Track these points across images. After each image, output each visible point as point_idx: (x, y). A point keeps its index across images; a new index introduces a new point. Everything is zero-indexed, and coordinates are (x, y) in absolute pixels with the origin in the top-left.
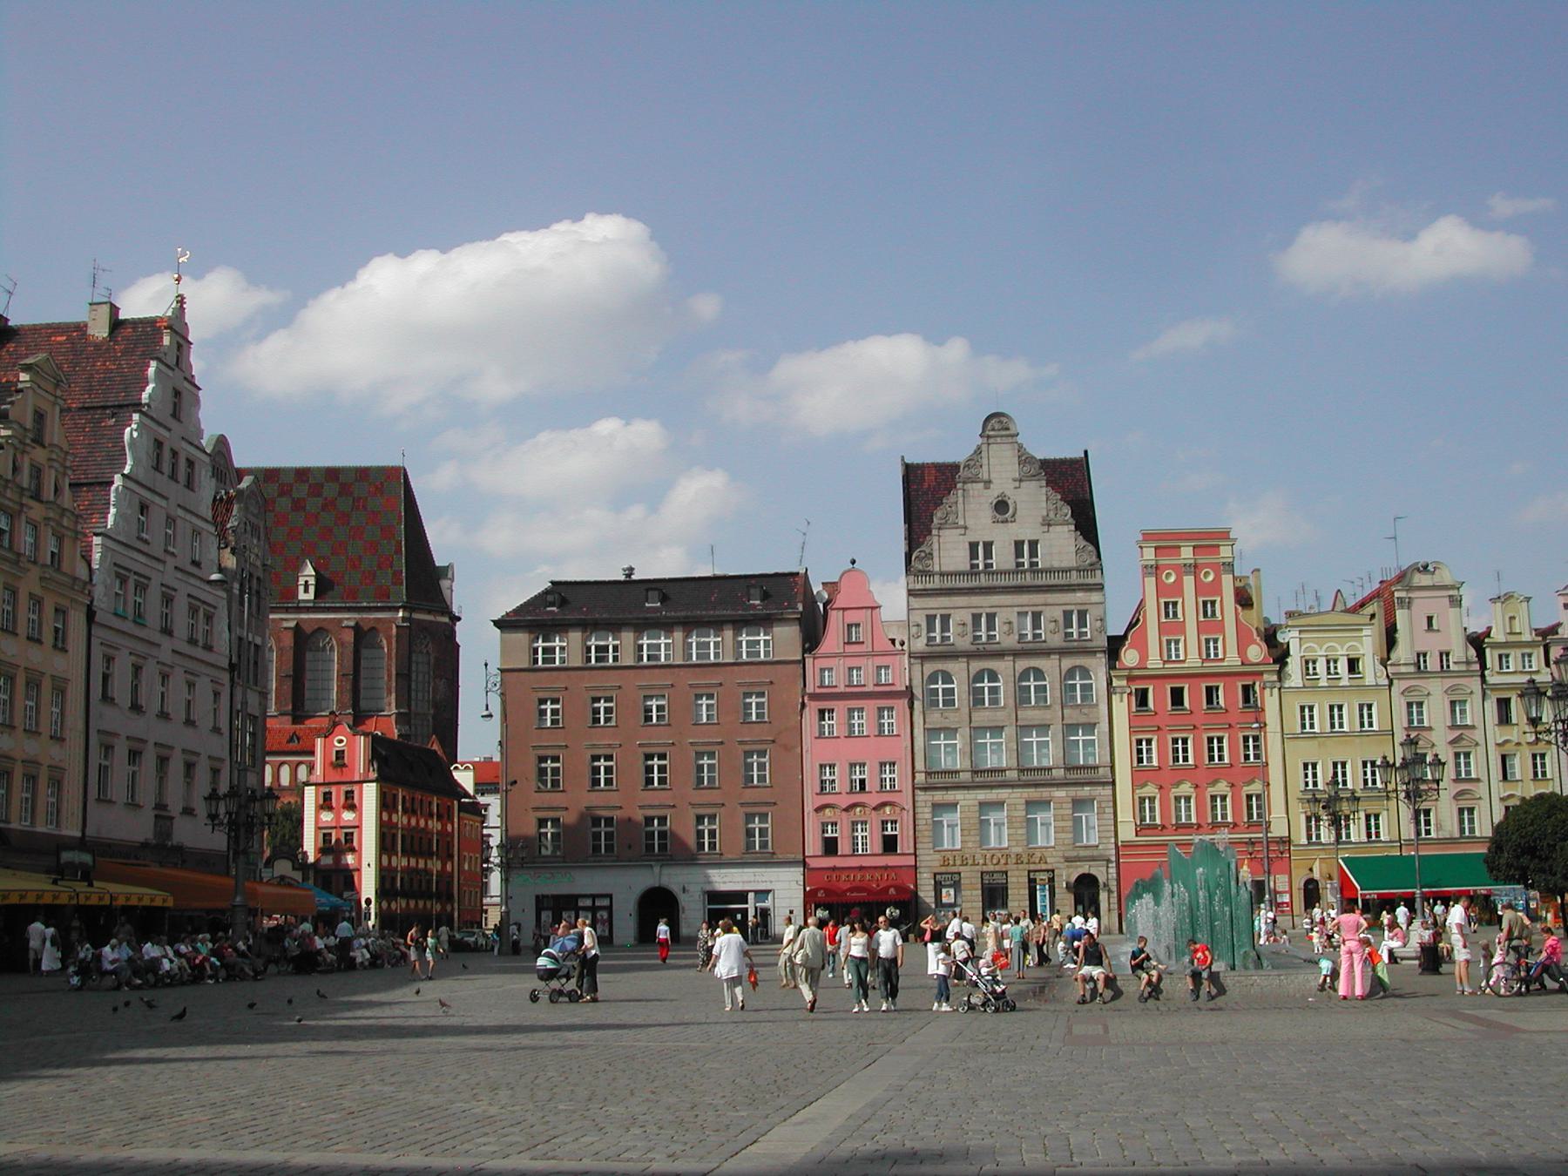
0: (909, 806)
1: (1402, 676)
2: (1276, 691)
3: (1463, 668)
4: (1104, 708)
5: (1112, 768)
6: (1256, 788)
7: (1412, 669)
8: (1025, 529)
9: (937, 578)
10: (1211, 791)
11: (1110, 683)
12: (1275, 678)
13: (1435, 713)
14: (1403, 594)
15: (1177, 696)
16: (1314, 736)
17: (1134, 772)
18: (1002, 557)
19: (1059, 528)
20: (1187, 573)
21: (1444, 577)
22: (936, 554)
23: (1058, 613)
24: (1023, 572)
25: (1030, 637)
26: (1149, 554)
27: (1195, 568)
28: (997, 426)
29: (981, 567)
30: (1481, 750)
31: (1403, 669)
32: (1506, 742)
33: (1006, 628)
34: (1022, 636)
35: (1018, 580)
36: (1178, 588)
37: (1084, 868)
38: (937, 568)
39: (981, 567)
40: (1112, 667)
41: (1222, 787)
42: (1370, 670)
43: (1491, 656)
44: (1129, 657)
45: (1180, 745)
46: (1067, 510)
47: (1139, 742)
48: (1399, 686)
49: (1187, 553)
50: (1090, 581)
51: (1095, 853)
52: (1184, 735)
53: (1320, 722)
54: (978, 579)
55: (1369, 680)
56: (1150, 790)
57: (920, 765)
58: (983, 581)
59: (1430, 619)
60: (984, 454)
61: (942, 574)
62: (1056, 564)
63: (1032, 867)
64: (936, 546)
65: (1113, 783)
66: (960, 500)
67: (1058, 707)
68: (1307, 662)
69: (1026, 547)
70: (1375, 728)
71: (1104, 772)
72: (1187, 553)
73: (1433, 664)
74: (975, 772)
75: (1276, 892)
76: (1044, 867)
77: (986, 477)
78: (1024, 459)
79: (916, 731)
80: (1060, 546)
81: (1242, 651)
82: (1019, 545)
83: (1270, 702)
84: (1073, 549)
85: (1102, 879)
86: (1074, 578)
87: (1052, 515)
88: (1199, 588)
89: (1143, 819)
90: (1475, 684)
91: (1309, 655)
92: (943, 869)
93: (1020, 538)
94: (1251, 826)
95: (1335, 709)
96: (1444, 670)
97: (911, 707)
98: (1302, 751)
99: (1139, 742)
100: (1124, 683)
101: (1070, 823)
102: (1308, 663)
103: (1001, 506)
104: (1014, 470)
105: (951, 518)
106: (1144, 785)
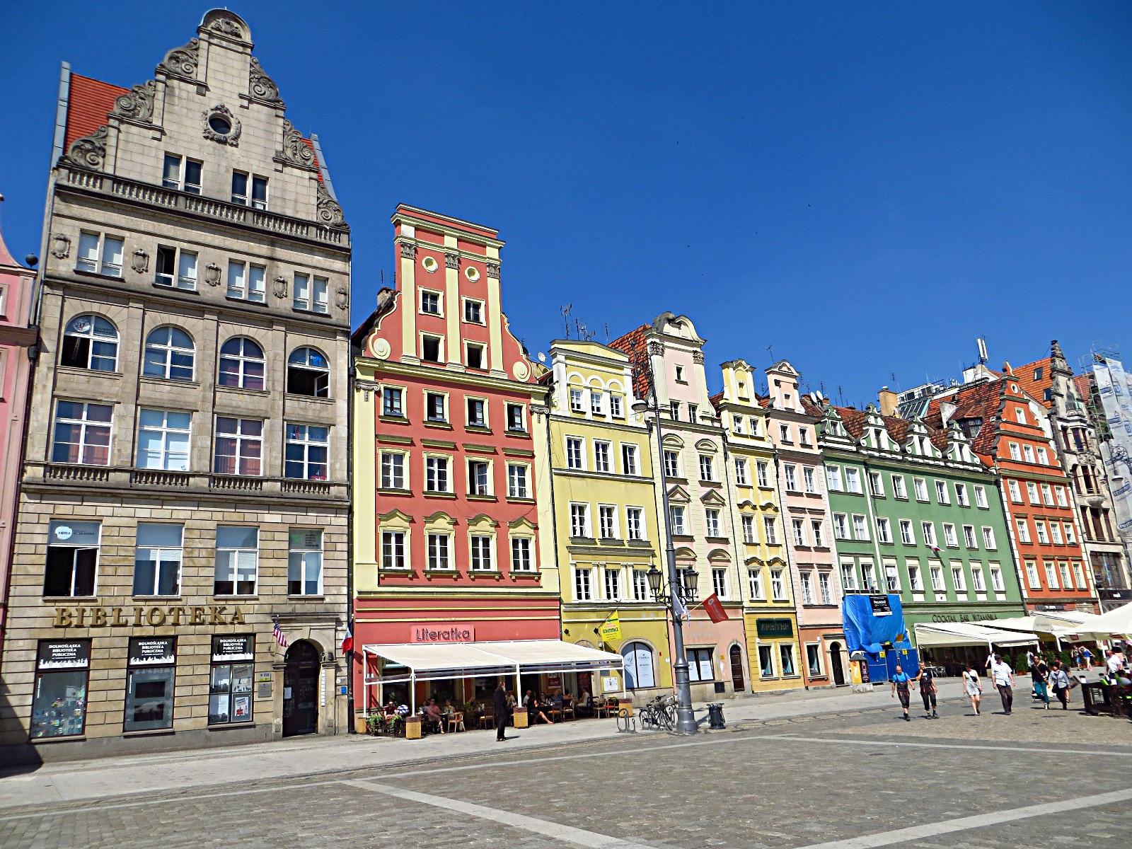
2: (543, 417)
3: (708, 423)
4: (342, 405)
5: (350, 488)
6: (523, 531)
9: (108, 183)
10: (472, 531)
11: (352, 375)
12: (543, 403)
13: (688, 465)
17: (382, 492)
18: (215, 183)
21: (689, 331)
22: (110, 151)
23: (287, 272)
28: (224, 27)
30: (727, 508)
35: (236, 218)
37: (303, 632)
38: (109, 170)
41: (484, 528)
43: (727, 416)
44: (379, 347)
45: (435, 468)
47: (386, 458)
52: (442, 455)
53: (588, 461)
54: (174, 200)
56: (397, 524)
57: (36, 452)
58: (182, 205)
59: (679, 370)
60: (202, 53)
61: (117, 180)
62: (289, 213)
63: (220, 630)
64: (112, 141)
65: (350, 511)
66: (160, 95)
72: (450, 242)
73: (684, 415)
74: (138, 474)
76: (240, 629)
77: (201, 78)
79: (36, 398)
81: (508, 368)
82: (239, 178)
83: (538, 428)
84: (315, 202)
85: (327, 647)
86: (313, 234)
87: (289, 153)
88: (463, 286)
90: (718, 440)
92: (60, 633)
93: (242, 168)
96: (692, 426)
97: (34, 360)
100: (372, 378)
101: (285, 563)
103: (219, 122)
105: (143, 113)
106: (391, 515)
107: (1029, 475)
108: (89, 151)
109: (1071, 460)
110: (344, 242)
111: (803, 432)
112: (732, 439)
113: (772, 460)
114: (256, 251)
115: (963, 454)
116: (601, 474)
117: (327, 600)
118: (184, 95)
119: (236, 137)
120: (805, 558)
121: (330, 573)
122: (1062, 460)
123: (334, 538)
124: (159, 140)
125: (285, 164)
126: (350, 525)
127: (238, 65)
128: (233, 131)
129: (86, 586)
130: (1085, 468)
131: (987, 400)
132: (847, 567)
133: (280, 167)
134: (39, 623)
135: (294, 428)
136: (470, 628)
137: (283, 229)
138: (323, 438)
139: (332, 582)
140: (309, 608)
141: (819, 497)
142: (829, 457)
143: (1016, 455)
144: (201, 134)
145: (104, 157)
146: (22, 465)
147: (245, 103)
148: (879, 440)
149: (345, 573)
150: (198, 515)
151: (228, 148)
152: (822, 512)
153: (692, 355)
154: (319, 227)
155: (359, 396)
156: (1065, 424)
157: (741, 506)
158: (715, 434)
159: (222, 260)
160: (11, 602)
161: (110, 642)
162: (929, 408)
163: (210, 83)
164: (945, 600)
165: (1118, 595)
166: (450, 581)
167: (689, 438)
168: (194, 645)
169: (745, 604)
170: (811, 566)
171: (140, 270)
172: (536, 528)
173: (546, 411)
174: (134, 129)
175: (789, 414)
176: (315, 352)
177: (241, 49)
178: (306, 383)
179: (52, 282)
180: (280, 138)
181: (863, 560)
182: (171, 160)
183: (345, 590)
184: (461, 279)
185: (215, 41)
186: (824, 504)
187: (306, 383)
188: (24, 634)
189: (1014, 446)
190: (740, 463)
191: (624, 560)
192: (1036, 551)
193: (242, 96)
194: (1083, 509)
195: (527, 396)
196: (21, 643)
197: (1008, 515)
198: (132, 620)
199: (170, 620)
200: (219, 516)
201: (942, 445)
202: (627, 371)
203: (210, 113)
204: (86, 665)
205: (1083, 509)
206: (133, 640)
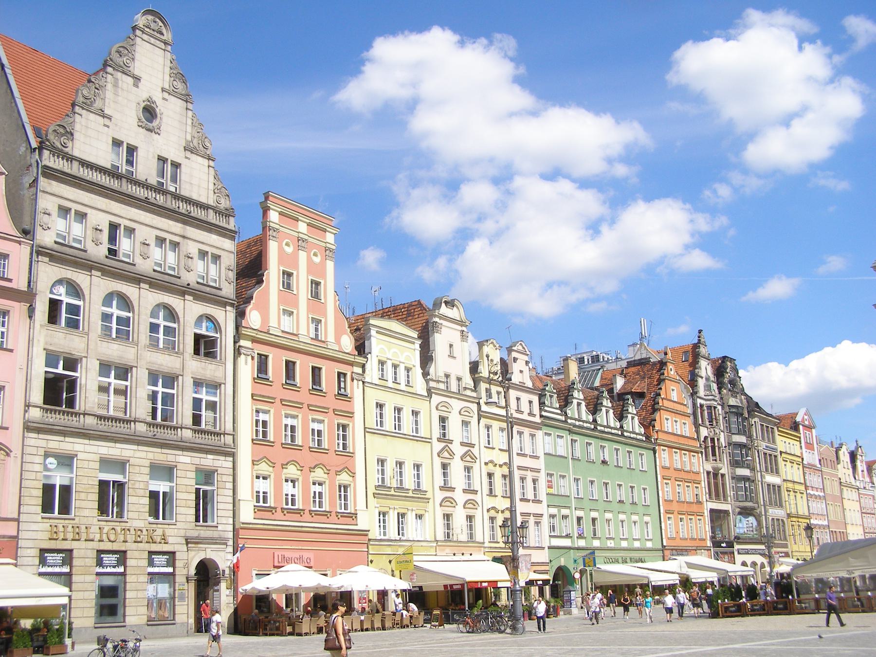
0: (16, 451)
2: (361, 383)
9: (76, 164)
19: (200, 159)
22: (76, 135)
23: (193, 249)
38: (76, 153)
44: (253, 318)
51: (215, 534)
61: (84, 163)
62: (195, 197)
65: (233, 455)
72: (302, 227)
76: (166, 548)
77: (137, 72)
86: (211, 217)
87: (195, 142)
90: (474, 407)
96: (459, 395)
98: (379, 446)
103: (149, 112)
105: (98, 104)
107: (677, 446)
108: (63, 135)
109: (704, 432)
110: (232, 224)
112: (484, 408)
114: (173, 230)
115: (633, 424)
116: (397, 434)
117: (220, 527)
118: (125, 86)
122: (698, 432)
124: (108, 127)
126: (234, 468)
127: (161, 60)
129: (65, 508)
130: (712, 440)
131: (649, 378)
132: (553, 516)
134: (40, 535)
136: (311, 555)
141: (537, 458)
142: (547, 423)
143: (668, 426)
145: (72, 140)
146: (28, 406)
148: (578, 411)
149: (231, 507)
150: (138, 454)
152: (538, 471)
153: (459, 334)
156: (703, 402)
157: (486, 464)
158: (473, 402)
159: (150, 235)
160: (23, 518)
161: (84, 554)
162: (602, 378)
164: (613, 545)
165: (724, 545)
166: (324, 519)
167: (457, 405)
168: (137, 561)
169: (487, 544)
171: (97, 243)
174: (92, 116)
175: (521, 388)
176: (209, 318)
177: (162, 46)
178: (205, 346)
179: (40, 251)
181: (565, 512)
182: (117, 143)
183: (231, 521)
184: (309, 259)
186: (540, 464)
187: (205, 346)
188: (29, 544)
189: (667, 419)
190: (488, 428)
191: (408, 504)
192: (675, 507)
193: (163, 90)
194: (708, 473)
196: (29, 551)
197: (659, 476)
198: (98, 537)
199: (122, 538)
200: (150, 456)
201: (621, 417)
202: (417, 346)
203: (143, 105)
204: (68, 570)
205: (708, 473)
206: (100, 552)
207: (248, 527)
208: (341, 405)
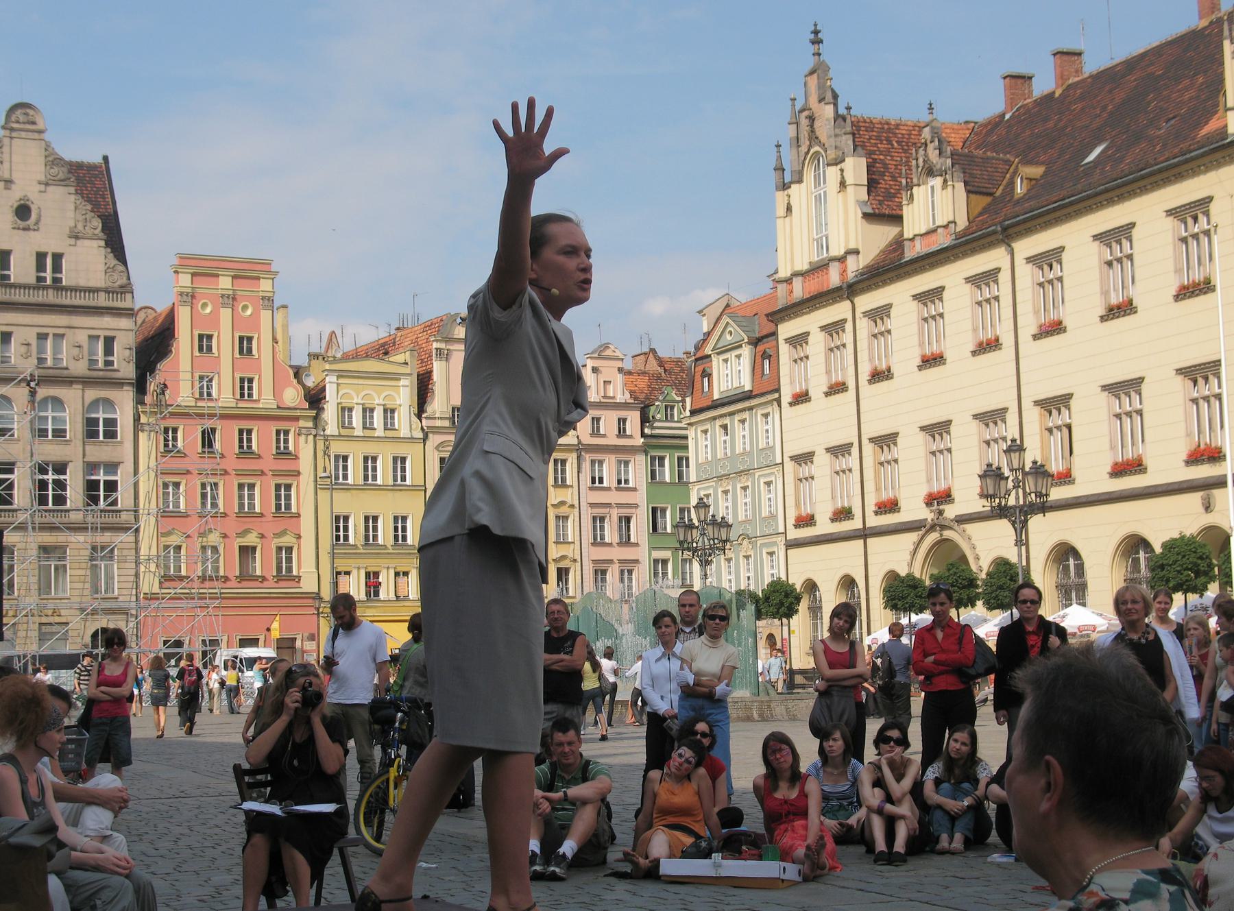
1: (438, 430)
2: (311, 438)
6: (287, 540)
7: (447, 423)
8: (49, 239)
11: (137, 419)
12: (310, 424)
14: (442, 346)
15: (208, 439)
16: (348, 488)
19: (87, 242)
20: (224, 305)
24: (46, 288)
25: (101, 365)
26: (185, 280)
27: (231, 300)
28: (22, 119)
29: (49, 282)
31: (438, 423)
32: (563, 503)
33: (23, 349)
34: (93, 362)
36: (214, 318)
39: (49, 282)
40: (140, 401)
42: (405, 422)
46: (98, 223)
47: (166, 486)
48: (434, 440)
49: (225, 283)
50: (119, 304)
52: (213, 480)
55: (404, 432)
62: (83, 283)
63: (44, 620)
65: (137, 530)
67: (80, 444)
68: (343, 409)
69: (49, 261)
70: (408, 482)
71: (126, 517)
72: (225, 283)
75: (303, 652)
76: (57, 619)
77: (6, 176)
78: (54, 160)
80: (87, 264)
81: (277, 393)
82: (41, 257)
83: (304, 449)
84: (103, 268)
86: (102, 300)
87: (80, 227)
89: (167, 567)
91: (346, 402)
94: (279, 578)
95: (370, 461)
99: (166, 486)
102: (345, 410)
103: (23, 211)
104: (38, 170)
106: (168, 534)
111: (622, 421)
113: (575, 455)
117: (121, 599)
119: (37, 223)
120: (602, 553)
121: (122, 579)
123: (125, 552)
125: (77, 238)
128: (34, 216)
133: (72, 241)
135: (92, 467)
137: (78, 301)
138: (115, 473)
139: (124, 585)
140: (107, 605)
144: (9, 226)
147: (42, 187)
149: (132, 579)
151: (31, 233)
154: (107, 291)
155: (143, 437)
163: (15, 177)
170: (611, 561)
172: (299, 537)
173: (314, 432)
180: (71, 214)
185: (14, 134)
191: (383, 562)
195: (297, 419)
200: (40, 539)
207: (152, 597)
208: (284, 465)
